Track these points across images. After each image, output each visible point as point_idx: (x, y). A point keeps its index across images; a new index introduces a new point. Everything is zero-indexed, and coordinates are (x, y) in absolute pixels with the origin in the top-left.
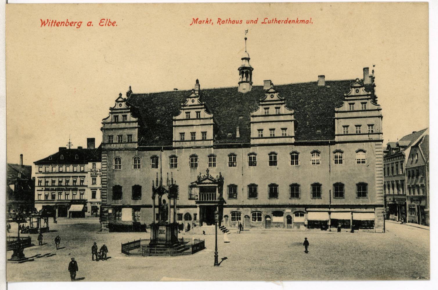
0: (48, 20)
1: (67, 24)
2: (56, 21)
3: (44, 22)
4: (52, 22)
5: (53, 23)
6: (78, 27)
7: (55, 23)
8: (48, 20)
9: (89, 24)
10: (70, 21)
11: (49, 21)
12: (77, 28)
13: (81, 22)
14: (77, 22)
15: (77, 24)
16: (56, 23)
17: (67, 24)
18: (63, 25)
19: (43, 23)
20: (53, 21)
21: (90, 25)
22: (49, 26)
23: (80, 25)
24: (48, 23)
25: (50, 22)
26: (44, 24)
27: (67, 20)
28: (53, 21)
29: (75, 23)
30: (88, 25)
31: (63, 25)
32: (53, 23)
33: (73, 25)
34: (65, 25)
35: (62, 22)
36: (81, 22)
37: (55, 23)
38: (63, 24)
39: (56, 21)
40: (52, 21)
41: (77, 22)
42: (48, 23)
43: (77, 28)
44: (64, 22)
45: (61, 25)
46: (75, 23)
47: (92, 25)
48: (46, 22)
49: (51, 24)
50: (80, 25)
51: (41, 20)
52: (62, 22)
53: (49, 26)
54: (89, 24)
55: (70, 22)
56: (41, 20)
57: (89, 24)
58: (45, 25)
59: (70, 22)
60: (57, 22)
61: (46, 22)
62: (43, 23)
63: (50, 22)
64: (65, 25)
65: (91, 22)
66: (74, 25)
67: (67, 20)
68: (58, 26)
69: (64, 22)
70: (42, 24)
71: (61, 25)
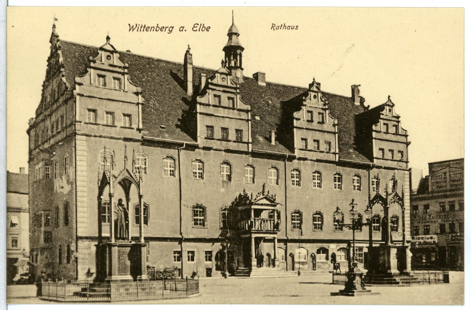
2: (145, 25)
3: (133, 26)
4: (141, 27)
5: (143, 28)
7: (145, 27)
9: (181, 29)
11: (138, 26)
12: (168, 33)
13: (173, 27)
14: (168, 27)
15: (167, 29)
16: (145, 28)
17: (158, 29)
19: (131, 28)
20: (142, 25)
21: (182, 30)
22: (137, 31)
23: (172, 30)
24: (137, 28)
25: (138, 27)
26: (132, 29)
27: (158, 25)
28: (142, 25)
30: (180, 31)
32: (143, 28)
33: (164, 30)
35: (152, 28)
36: (173, 27)
38: (153, 28)
39: (145, 25)
40: (141, 26)
41: (168, 27)
42: (137, 28)
43: (168, 33)
45: (150, 31)
46: (166, 28)
48: (134, 27)
49: (140, 28)
50: (172, 30)
51: (129, 25)
52: (152, 28)
53: (137, 31)
54: (182, 29)
56: (129, 25)
57: (182, 29)
58: (133, 30)
60: (146, 26)
62: (131, 28)
63: (138, 27)
65: (184, 27)
66: (165, 31)
67: (158, 25)
68: (148, 31)
69: (154, 27)
70: (130, 30)
71: (150, 31)
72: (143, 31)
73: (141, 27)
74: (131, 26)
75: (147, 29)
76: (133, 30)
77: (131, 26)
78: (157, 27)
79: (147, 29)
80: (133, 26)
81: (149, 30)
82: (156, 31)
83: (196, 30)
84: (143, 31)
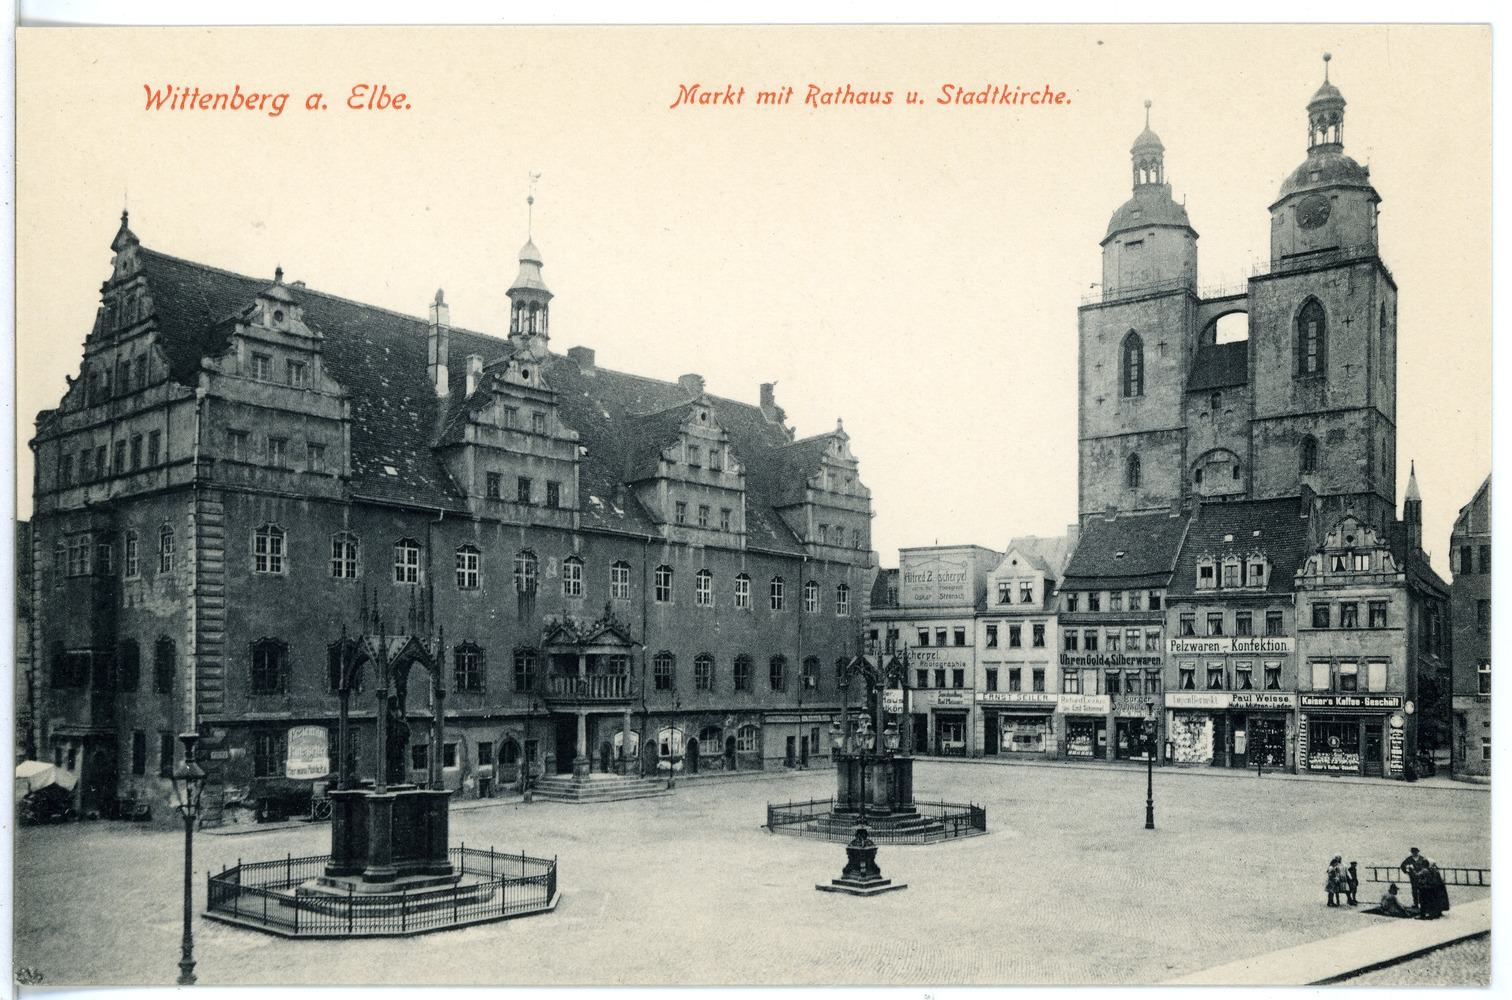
1: (238, 101)
2: (197, 90)
4: (185, 96)
5: (189, 99)
7: (196, 95)
16: (198, 99)
18: (224, 107)
20: (187, 90)
31: (224, 107)
32: (189, 99)
34: (228, 104)
35: (218, 97)
37: (196, 95)
38: (222, 100)
39: (197, 90)
44: (226, 97)
45: (214, 107)
52: (218, 97)
60: (202, 93)
64: (228, 104)
68: (206, 107)
71: (214, 107)
72: (192, 106)
73: (185, 96)
75: (202, 101)
78: (236, 94)
79: (202, 101)
81: (211, 104)
82: (233, 106)
84: (192, 106)
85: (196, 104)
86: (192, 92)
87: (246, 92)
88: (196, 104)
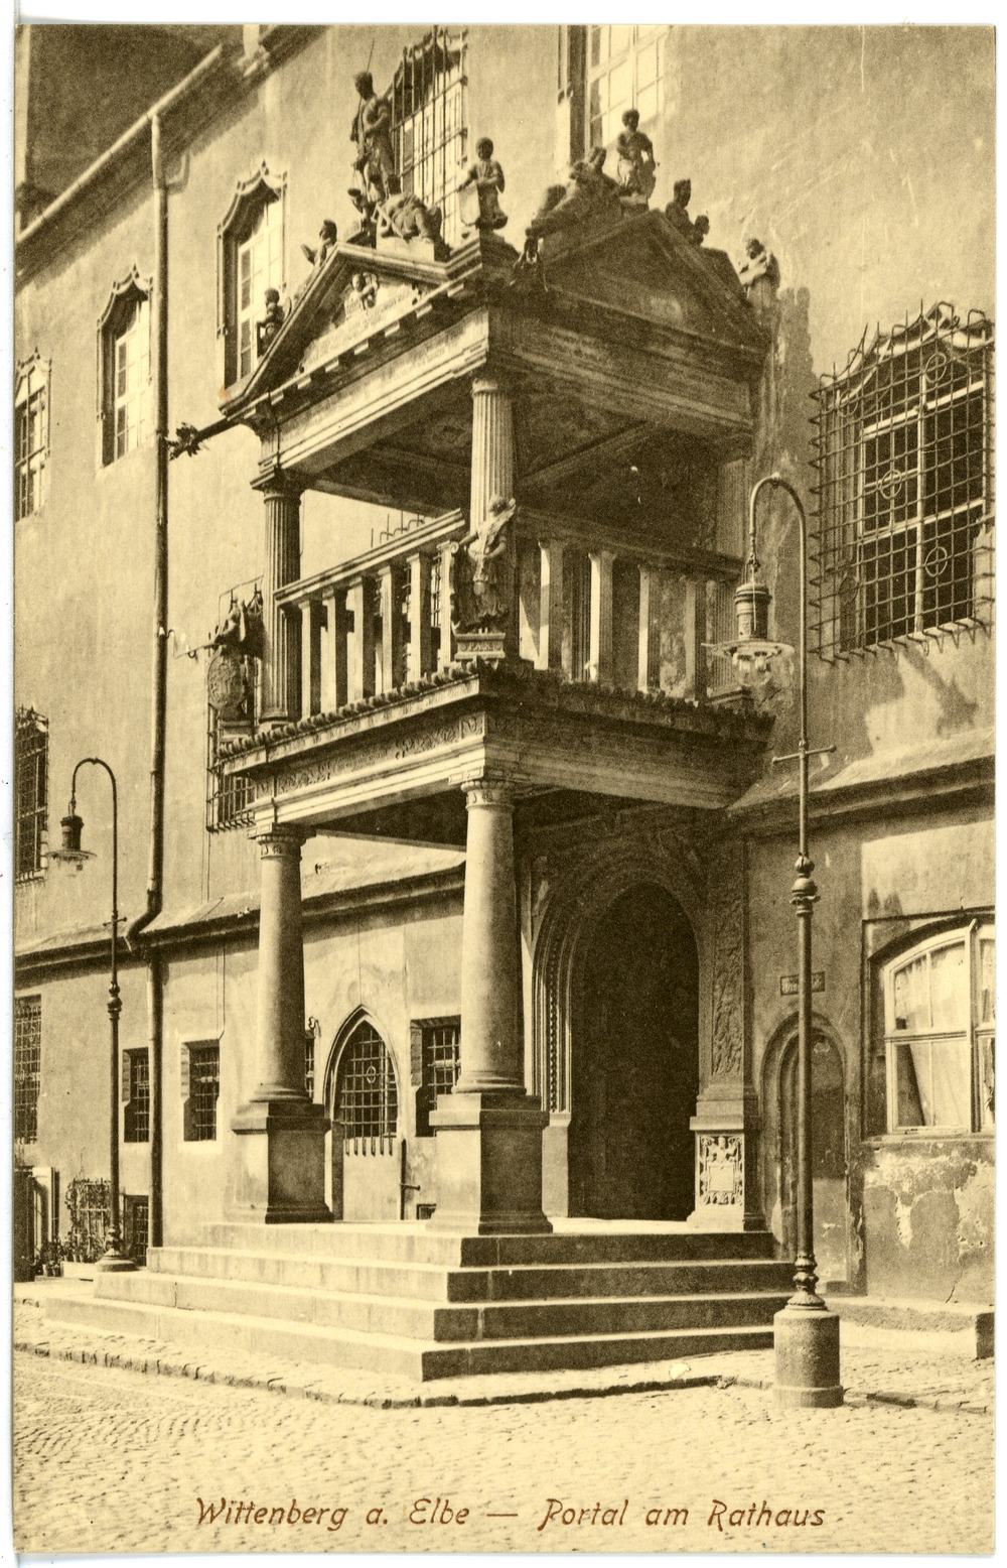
0: (223, 1501)
3: (212, 1508)
4: (240, 1510)
6: (333, 1526)
8: (223, 1501)
9: (374, 1515)
10: (303, 1507)
12: (330, 1529)
13: (345, 1511)
15: (327, 1516)
16: (253, 1513)
17: (293, 1519)
21: (377, 1521)
24: (226, 1511)
26: (209, 1515)
29: (322, 1511)
32: (244, 1513)
34: (285, 1520)
36: (345, 1511)
37: (251, 1509)
42: (226, 1511)
43: (330, 1529)
46: (322, 1511)
47: (385, 1522)
49: (234, 1513)
51: (200, 1500)
52: (274, 1511)
54: (375, 1517)
55: (303, 1510)
56: (200, 1500)
58: (213, 1518)
59: (303, 1510)
61: (218, 1505)
69: (282, 1510)
74: (207, 1505)
76: (213, 1518)
77: (207, 1505)
80: (212, 1508)
81: (266, 1519)
82: (289, 1521)
83: (423, 1521)
85: (251, 1519)
86: (247, 1504)
87: (303, 1507)
88: (251, 1519)
